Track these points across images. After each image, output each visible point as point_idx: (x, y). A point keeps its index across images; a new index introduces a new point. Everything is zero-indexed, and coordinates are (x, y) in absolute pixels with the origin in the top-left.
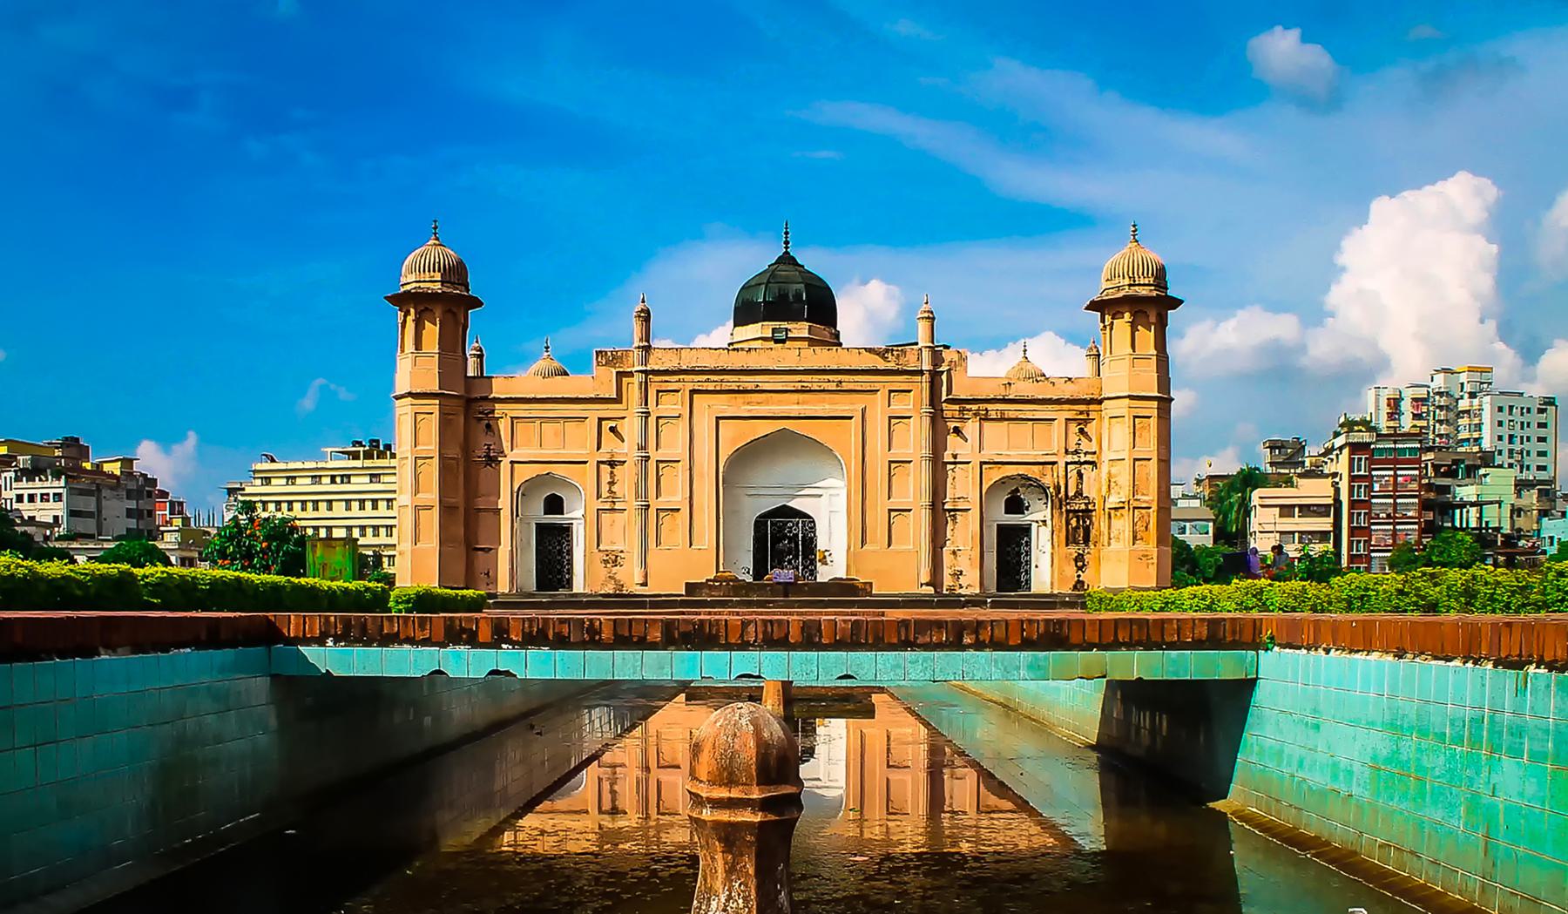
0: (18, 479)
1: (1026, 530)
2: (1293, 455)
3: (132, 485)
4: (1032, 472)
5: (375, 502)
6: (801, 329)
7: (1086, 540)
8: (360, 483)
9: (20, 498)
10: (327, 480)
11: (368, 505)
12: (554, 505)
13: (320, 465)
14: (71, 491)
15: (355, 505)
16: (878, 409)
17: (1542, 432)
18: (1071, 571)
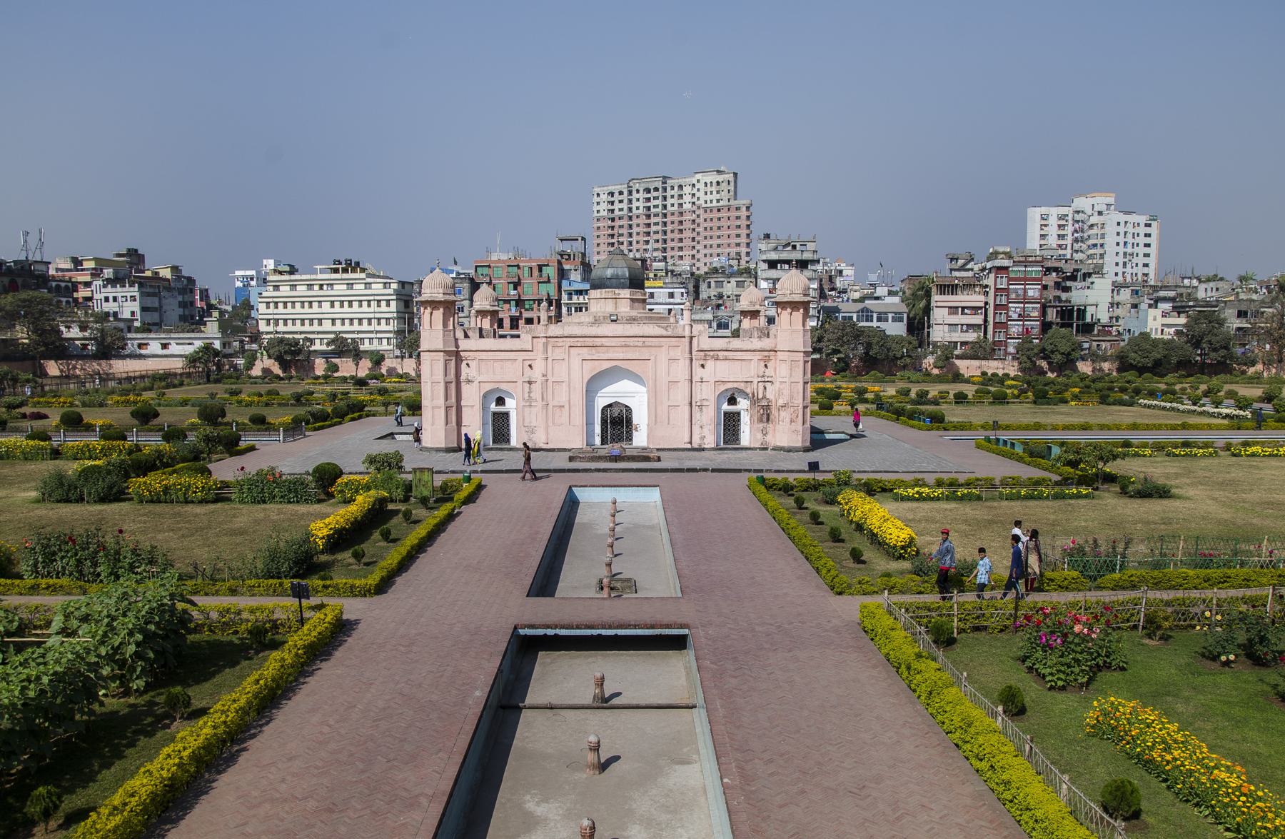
0: (105, 286)
1: (738, 414)
2: (965, 264)
3: (179, 285)
4: (741, 386)
5: (350, 303)
6: (626, 293)
7: (768, 420)
8: (340, 289)
9: (107, 299)
10: (316, 287)
11: (346, 304)
12: (500, 401)
13: (313, 277)
14: (142, 294)
15: (337, 304)
16: (663, 355)
17: (1147, 240)
18: (760, 436)
